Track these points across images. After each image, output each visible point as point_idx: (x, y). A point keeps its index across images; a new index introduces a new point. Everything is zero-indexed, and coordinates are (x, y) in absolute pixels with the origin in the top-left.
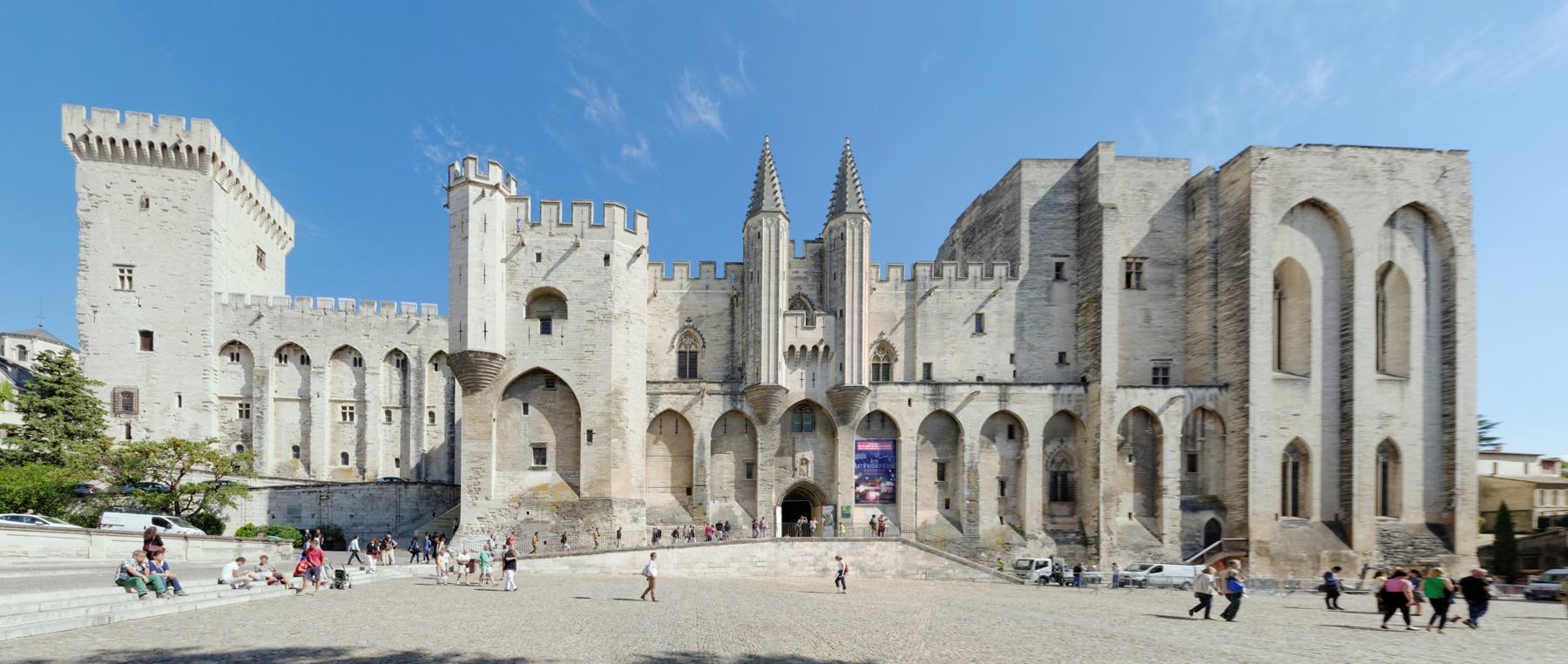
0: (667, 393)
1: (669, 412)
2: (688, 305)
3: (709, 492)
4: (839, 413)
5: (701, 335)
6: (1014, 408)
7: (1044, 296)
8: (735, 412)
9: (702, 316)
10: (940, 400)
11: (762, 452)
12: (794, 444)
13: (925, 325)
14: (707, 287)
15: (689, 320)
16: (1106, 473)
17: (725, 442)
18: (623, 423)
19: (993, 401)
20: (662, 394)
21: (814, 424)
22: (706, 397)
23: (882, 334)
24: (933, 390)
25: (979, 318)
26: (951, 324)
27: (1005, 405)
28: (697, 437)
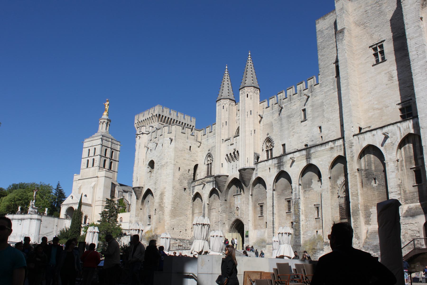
0: (196, 186)
6: (314, 161)
7: (333, 87)
9: (212, 147)
12: (234, 201)
13: (281, 124)
15: (209, 151)
16: (352, 195)
18: (163, 205)
19: (304, 160)
20: (195, 186)
22: (206, 184)
23: (268, 134)
24: (278, 161)
25: (304, 110)
26: (292, 120)
27: (309, 161)
28: (203, 203)
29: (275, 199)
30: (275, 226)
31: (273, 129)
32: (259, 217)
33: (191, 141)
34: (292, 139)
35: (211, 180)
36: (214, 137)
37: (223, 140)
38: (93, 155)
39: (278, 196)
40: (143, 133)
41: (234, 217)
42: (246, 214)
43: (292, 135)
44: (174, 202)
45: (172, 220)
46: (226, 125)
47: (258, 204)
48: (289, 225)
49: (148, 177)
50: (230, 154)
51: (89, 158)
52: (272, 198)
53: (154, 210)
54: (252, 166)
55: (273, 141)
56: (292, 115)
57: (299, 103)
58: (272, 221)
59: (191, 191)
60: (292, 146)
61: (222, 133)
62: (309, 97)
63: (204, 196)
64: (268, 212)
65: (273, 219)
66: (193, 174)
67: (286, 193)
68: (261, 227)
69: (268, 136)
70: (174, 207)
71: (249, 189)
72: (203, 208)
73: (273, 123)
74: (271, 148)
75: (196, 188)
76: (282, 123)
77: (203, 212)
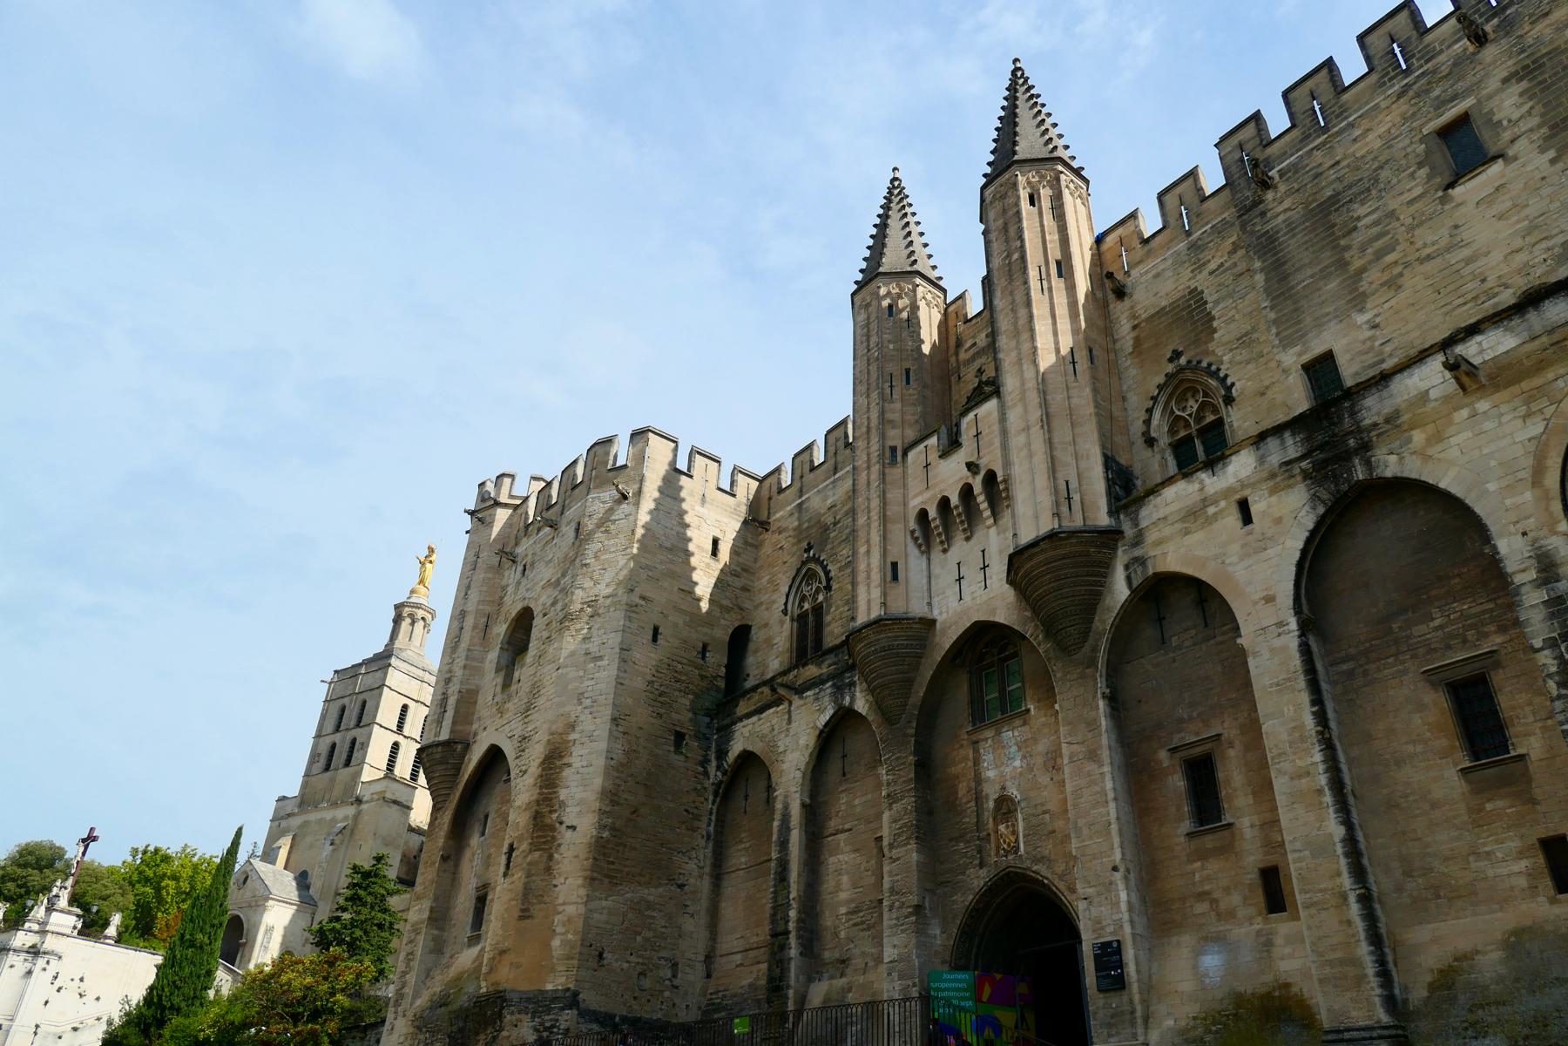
1: (748, 758)
2: (809, 521)
3: (793, 952)
4: (1050, 627)
5: (824, 568)
8: (844, 719)
10: (1345, 457)
11: (890, 810)
14: (836, 470)
15: (807, 551)
17: (844, 799)
18: (555, 816)
20: (734, 723)
21: (1023, 684)
23: (1176, 355)
28: (779, 806)
29: (1324, 686)
30: (1379, 881)
31: (1213, 318)
32: (1190, 835)
33: (719, 518)
34: (1386, 306)
35: (825, 670)
36: (834, 482)
37: (893, 449)
38: (353, 723)
39: (1345, 667)
40: (497, 504)
41: (981, 865)
42: (1081, 822)
43: (1382, 285)
44: (611, 796)
45: (595, 904)
46: (908, 382)
47: (1173, 750)
48: (1523, 864)
49: (499, 689)
50: (944, 503)
51: (337, 737)
52: (1301, 682)
53: (505, 849)
54: (1103, 519)
55: (1222, 374)
56: (1354, 190)
57: (1404, 108)
58: (1339, 849)
59: (713, 749)
60: (1388, 349)
61: (889, 416)
62: (1480, 39)
63: (784, 767)
64: (1280, 785)
65: (1348, 823)
66: (724, 669)
67: (1419, 629)
68: (1223, 906)
69: (1183, 361)
70: (613, 829)
71: (1092, 663)
72: (775, 830)
73: (1202, 292)
74: (1210, 418)
75: (737, 735)
76: (1278, 259)
77: (774, 855)
